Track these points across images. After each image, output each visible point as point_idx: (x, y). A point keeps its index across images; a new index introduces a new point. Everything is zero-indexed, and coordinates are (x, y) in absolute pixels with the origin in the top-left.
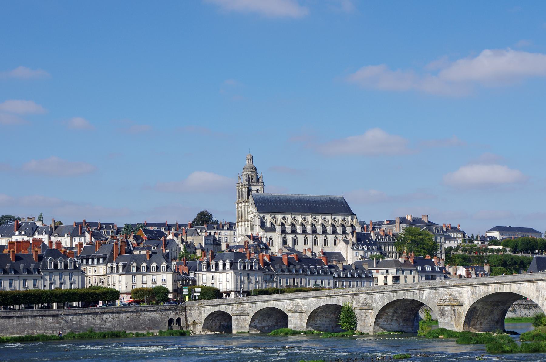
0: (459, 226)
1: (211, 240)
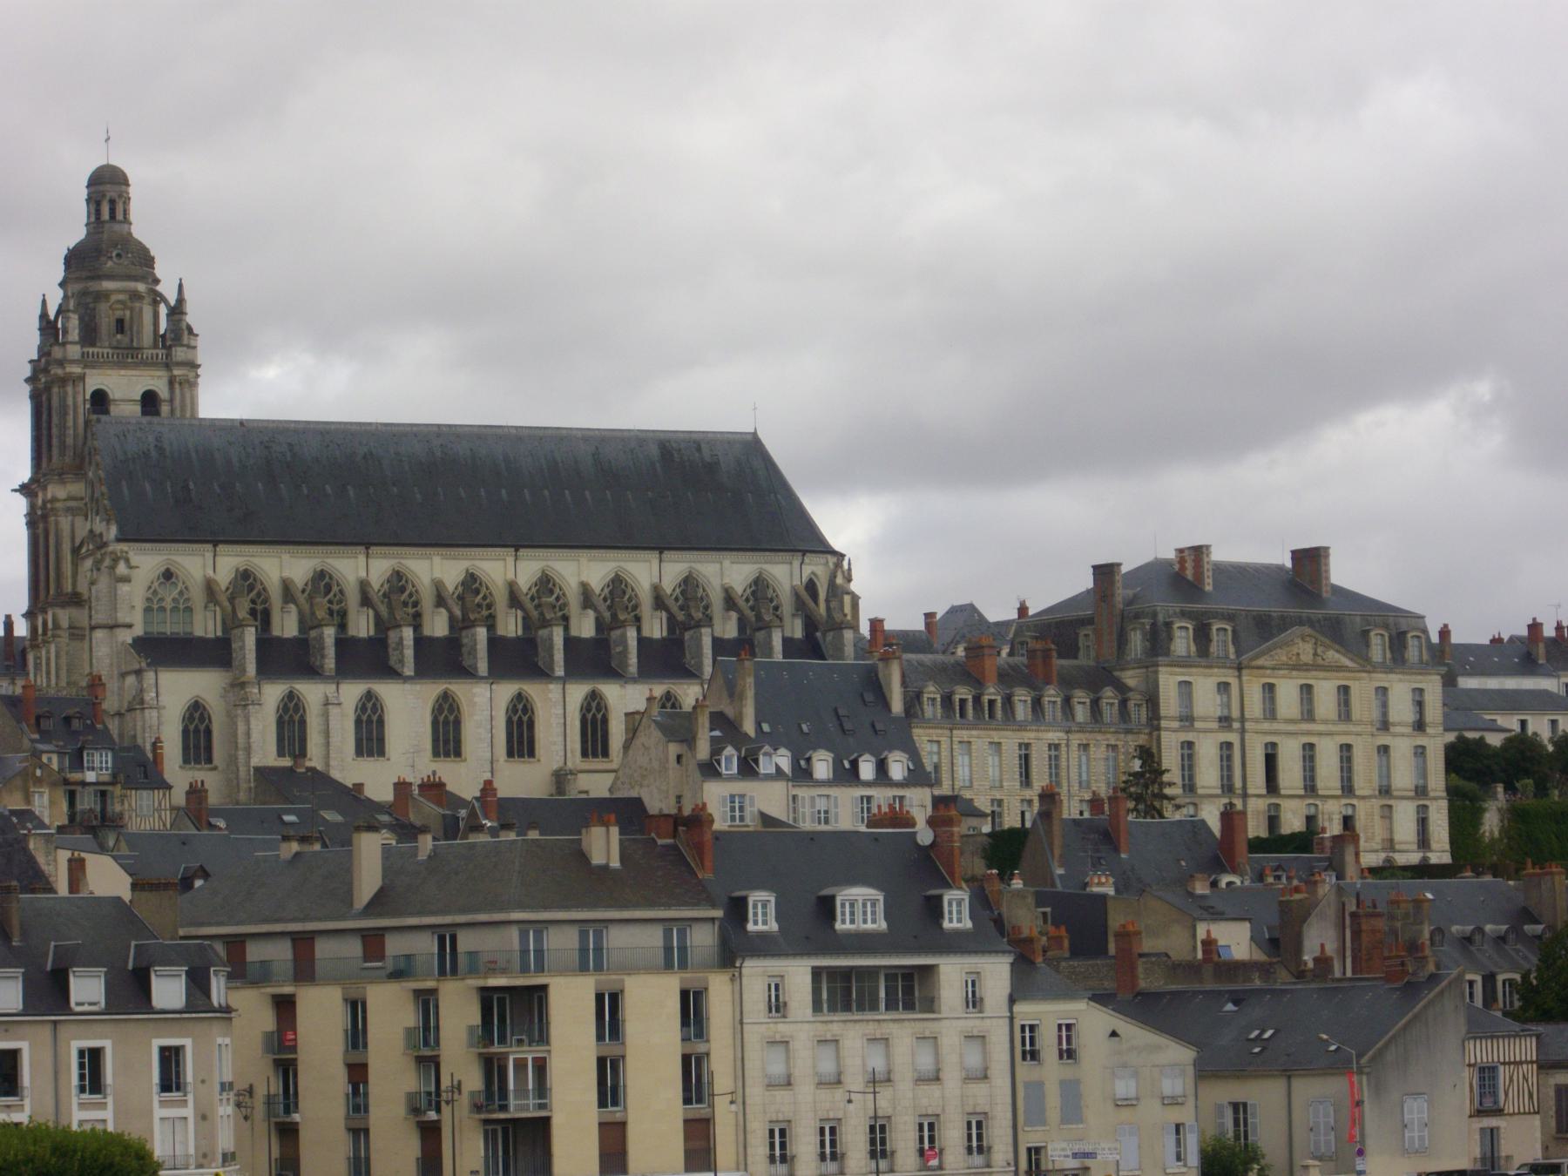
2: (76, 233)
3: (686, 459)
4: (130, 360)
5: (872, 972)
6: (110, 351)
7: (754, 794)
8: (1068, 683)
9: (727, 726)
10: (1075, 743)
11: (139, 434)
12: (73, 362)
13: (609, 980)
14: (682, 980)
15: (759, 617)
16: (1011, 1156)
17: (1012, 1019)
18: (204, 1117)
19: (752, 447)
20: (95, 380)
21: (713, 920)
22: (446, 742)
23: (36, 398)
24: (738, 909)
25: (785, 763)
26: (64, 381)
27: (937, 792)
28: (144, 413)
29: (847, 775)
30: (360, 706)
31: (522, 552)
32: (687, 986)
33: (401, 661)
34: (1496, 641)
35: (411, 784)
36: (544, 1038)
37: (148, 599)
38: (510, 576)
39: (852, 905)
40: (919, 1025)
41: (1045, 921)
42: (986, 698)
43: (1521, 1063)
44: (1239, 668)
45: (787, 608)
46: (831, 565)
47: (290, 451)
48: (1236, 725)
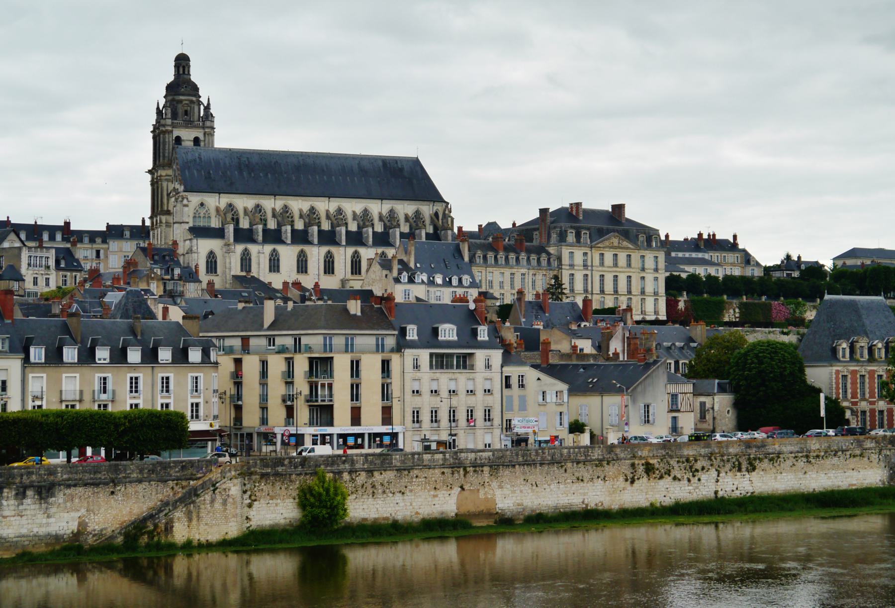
0: (735, 237)
1: (48, 258)
2: (170, 77)
5: (451, 355)
8: (529, 251)
9: (404, 265)
10: (531, 273)
11: (192, 153)
12: (168, 125)
13: (356, 356)
14: (382, 356)
15: (417, 225)
16: (500, 422)
17: (502, 373)
18: (207, 402)
19: (416, 164)
20: (177, 133)
21: (394, 335)
22: (302, 268)
23: (154, 138)
24: (403, 332)
25: (425, 279)
26: (164, 132)
27: (480, 290)
28: (195, 145)
29: (448, 284)
31: (331, 199)
32: (384, 359)
33: (286, 238)
34: (686, 240)
35: (288, 283)
36: (331, 376)
37: (195, 213)
38: (327, 208)
39: (445, 331)
40: (468, 374)
41: (517, 338)
42: (499, 256)
43: (687, 393)
44: (591, 248)
45: (428, 222)
46: (444, 206)
48: (590, 268)
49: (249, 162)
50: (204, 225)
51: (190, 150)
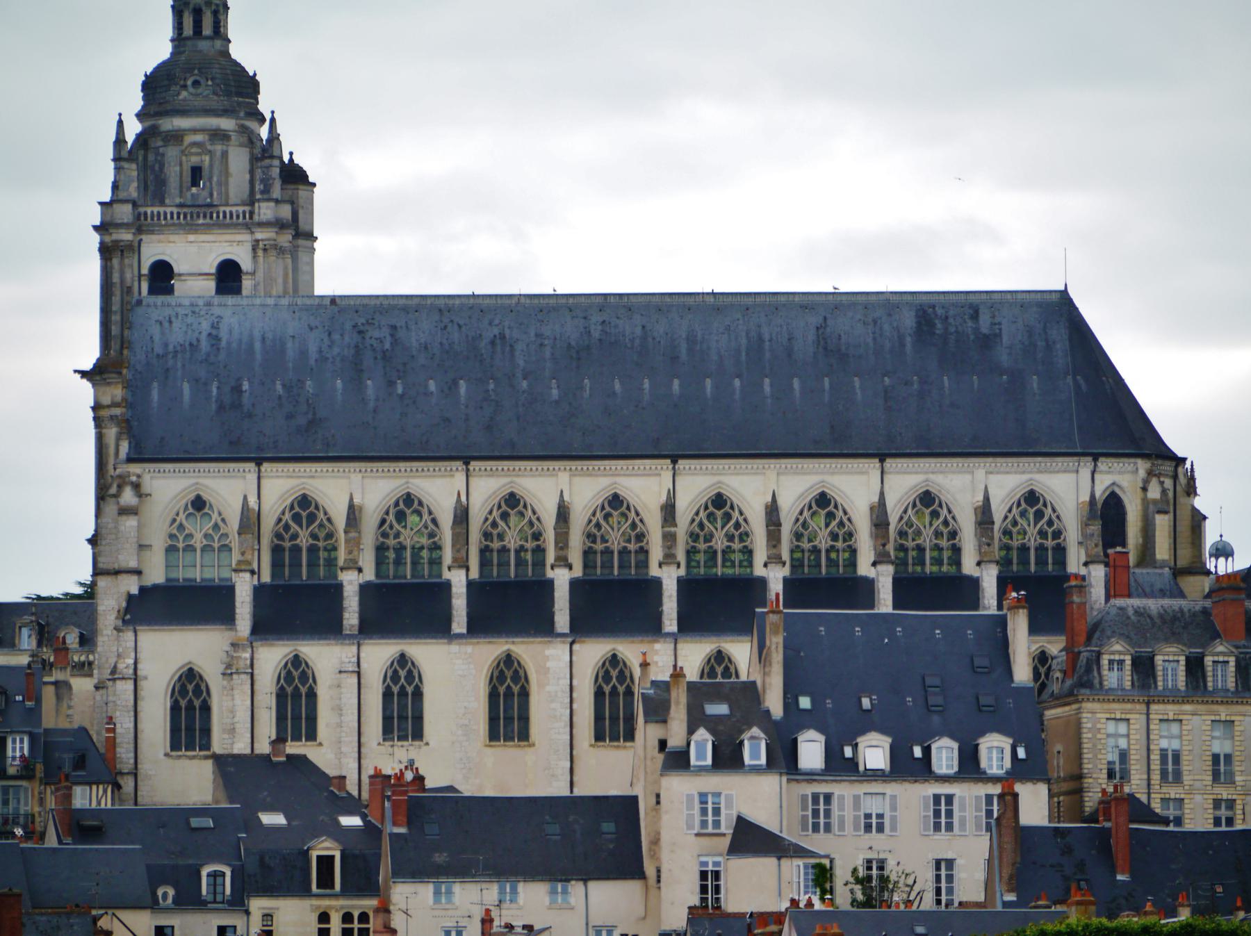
3: (952, 330)
4: (201, 221)
6: (175, 210)
7: (733, 793)
11: (190, 320)
20: (154, 249)
22: (508, 719)
30: (389, 675)
31: (682, 463)
37: (172, 536)
46: (1142, 473)
47: (392, 335)
49: (395, 342)
50: (207, 575)
51: (181, 311)
